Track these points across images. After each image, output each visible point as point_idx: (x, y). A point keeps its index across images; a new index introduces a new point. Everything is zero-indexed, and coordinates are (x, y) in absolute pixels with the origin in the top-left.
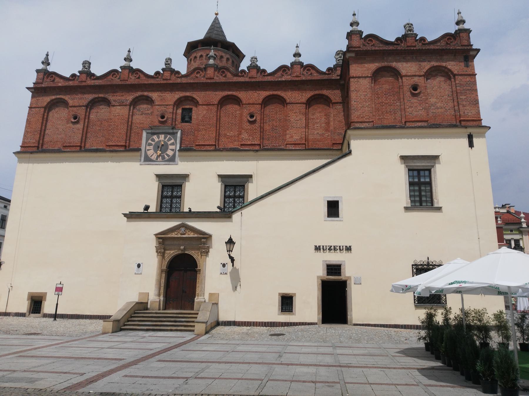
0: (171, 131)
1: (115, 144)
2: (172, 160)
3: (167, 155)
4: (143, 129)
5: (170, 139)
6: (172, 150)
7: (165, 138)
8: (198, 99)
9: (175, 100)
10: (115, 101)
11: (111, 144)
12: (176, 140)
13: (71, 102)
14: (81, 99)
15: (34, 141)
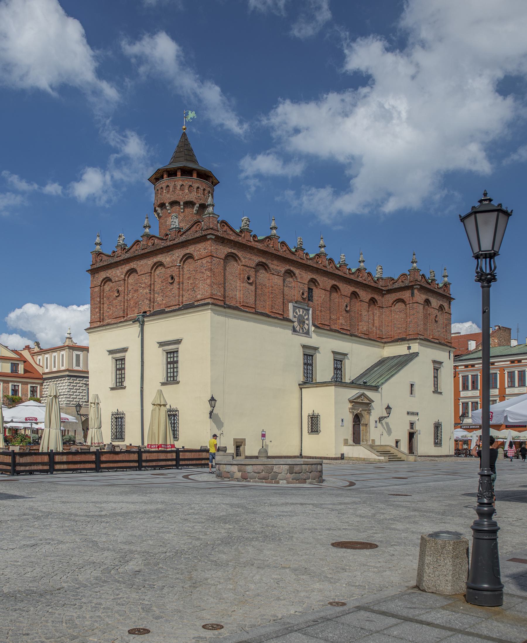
0: (306, 308)
1: (277, 312)
2: (307, 333)
3: (304, 327)
4: (291, 301)
5: (305, 315)
6: (307, 324)
7: (303, 312)
8: (320, 283)
9: (308, 280)
10: (273, 269)
11: (275, 311)
12: (308, 316)
13: (244, 261)
14: (250, 259)
15: (220, 294)
